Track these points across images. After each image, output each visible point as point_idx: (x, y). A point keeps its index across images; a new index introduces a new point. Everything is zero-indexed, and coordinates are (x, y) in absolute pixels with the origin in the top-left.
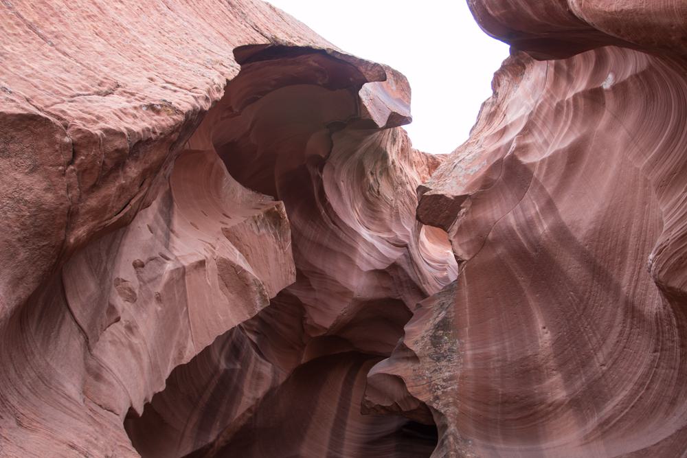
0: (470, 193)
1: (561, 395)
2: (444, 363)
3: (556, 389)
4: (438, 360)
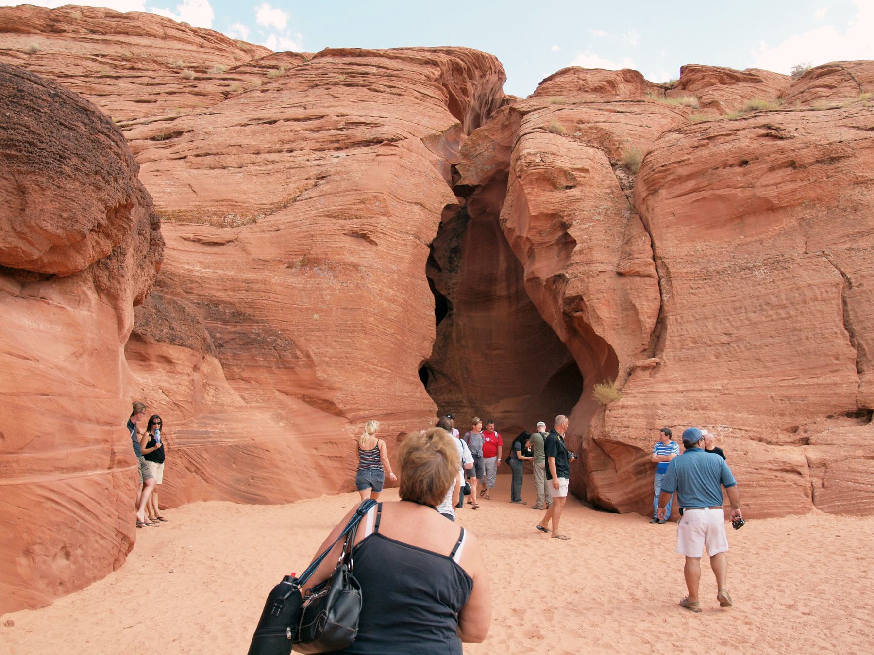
0: (482, 184)
1: (504, 293)
2: (454, 274)
3: (501, 289)
4: (451, 272)
